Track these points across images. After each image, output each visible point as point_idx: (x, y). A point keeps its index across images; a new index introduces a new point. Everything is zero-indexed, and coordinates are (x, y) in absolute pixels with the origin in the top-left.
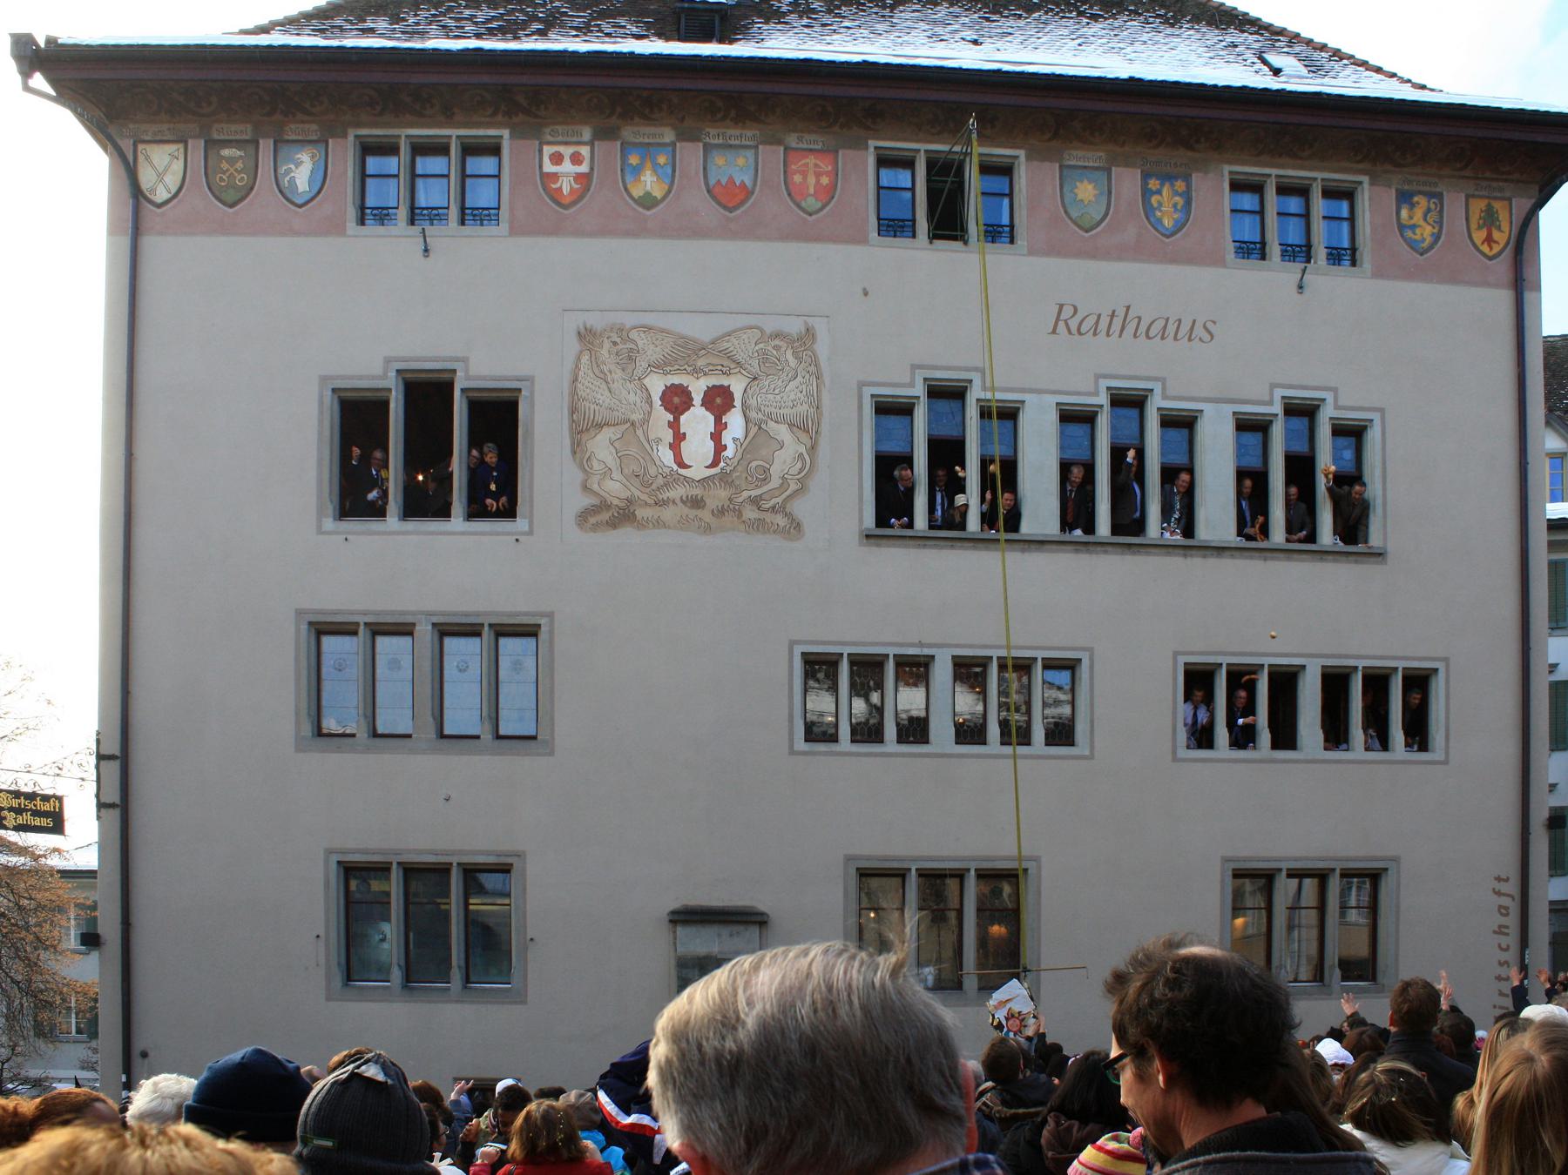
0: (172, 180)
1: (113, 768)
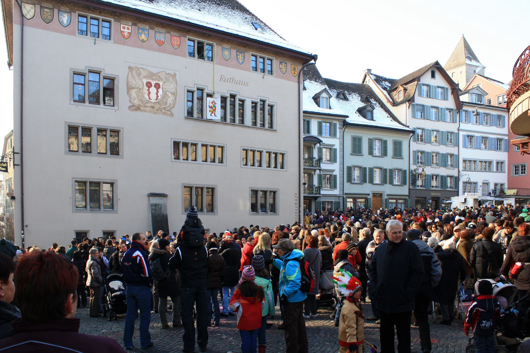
1: (18, 157)
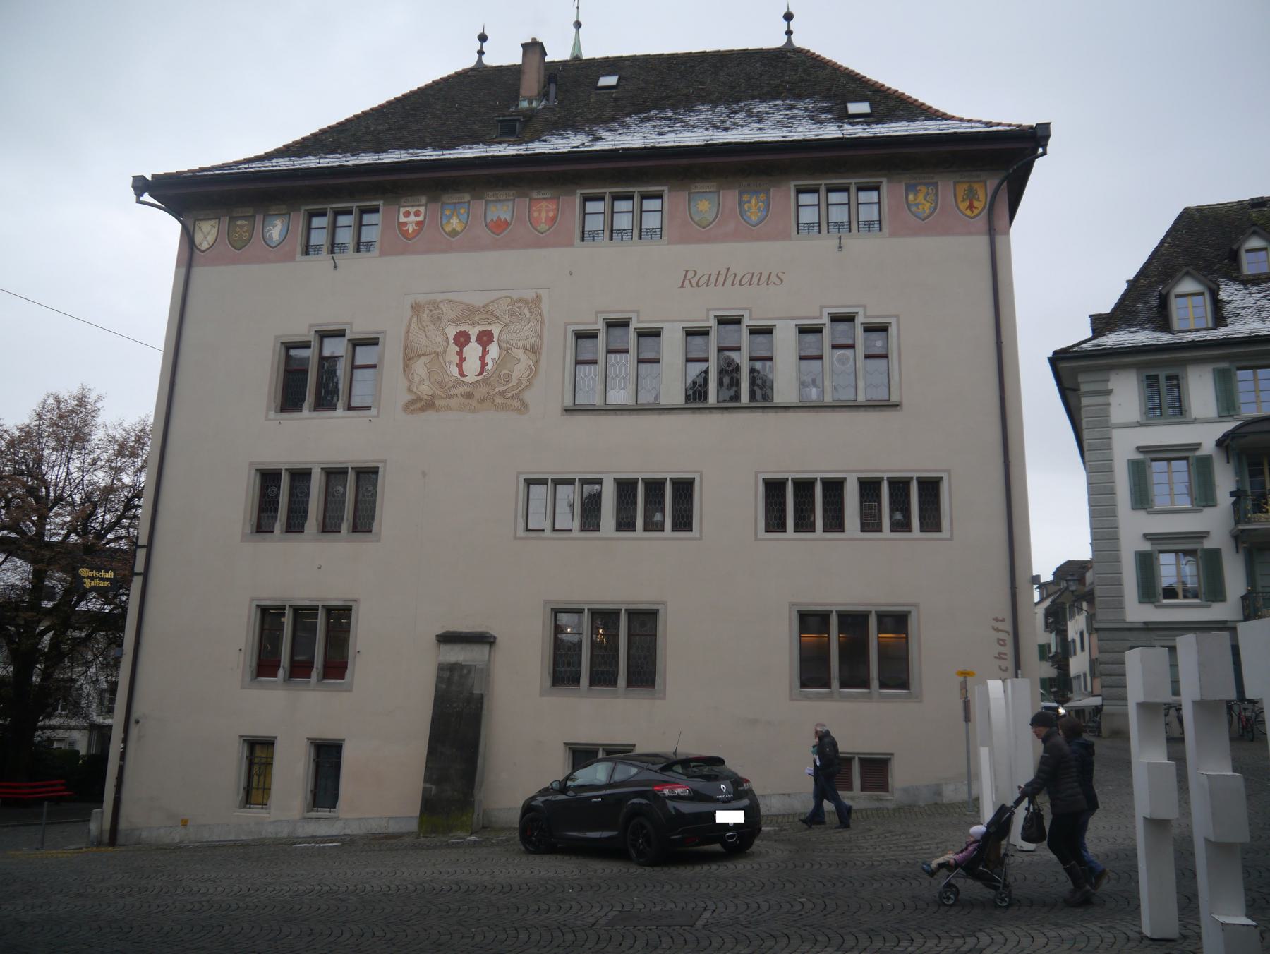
0: (211, 239)
